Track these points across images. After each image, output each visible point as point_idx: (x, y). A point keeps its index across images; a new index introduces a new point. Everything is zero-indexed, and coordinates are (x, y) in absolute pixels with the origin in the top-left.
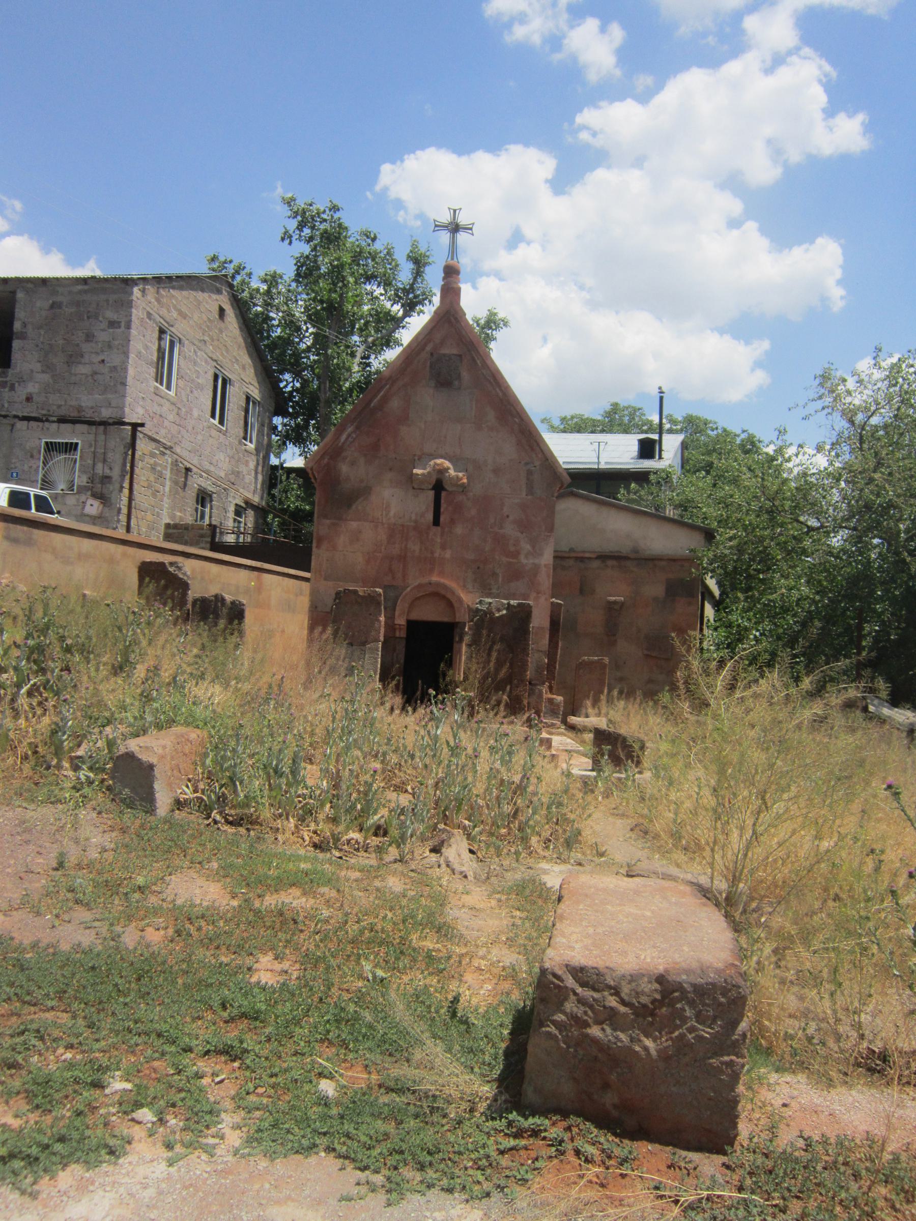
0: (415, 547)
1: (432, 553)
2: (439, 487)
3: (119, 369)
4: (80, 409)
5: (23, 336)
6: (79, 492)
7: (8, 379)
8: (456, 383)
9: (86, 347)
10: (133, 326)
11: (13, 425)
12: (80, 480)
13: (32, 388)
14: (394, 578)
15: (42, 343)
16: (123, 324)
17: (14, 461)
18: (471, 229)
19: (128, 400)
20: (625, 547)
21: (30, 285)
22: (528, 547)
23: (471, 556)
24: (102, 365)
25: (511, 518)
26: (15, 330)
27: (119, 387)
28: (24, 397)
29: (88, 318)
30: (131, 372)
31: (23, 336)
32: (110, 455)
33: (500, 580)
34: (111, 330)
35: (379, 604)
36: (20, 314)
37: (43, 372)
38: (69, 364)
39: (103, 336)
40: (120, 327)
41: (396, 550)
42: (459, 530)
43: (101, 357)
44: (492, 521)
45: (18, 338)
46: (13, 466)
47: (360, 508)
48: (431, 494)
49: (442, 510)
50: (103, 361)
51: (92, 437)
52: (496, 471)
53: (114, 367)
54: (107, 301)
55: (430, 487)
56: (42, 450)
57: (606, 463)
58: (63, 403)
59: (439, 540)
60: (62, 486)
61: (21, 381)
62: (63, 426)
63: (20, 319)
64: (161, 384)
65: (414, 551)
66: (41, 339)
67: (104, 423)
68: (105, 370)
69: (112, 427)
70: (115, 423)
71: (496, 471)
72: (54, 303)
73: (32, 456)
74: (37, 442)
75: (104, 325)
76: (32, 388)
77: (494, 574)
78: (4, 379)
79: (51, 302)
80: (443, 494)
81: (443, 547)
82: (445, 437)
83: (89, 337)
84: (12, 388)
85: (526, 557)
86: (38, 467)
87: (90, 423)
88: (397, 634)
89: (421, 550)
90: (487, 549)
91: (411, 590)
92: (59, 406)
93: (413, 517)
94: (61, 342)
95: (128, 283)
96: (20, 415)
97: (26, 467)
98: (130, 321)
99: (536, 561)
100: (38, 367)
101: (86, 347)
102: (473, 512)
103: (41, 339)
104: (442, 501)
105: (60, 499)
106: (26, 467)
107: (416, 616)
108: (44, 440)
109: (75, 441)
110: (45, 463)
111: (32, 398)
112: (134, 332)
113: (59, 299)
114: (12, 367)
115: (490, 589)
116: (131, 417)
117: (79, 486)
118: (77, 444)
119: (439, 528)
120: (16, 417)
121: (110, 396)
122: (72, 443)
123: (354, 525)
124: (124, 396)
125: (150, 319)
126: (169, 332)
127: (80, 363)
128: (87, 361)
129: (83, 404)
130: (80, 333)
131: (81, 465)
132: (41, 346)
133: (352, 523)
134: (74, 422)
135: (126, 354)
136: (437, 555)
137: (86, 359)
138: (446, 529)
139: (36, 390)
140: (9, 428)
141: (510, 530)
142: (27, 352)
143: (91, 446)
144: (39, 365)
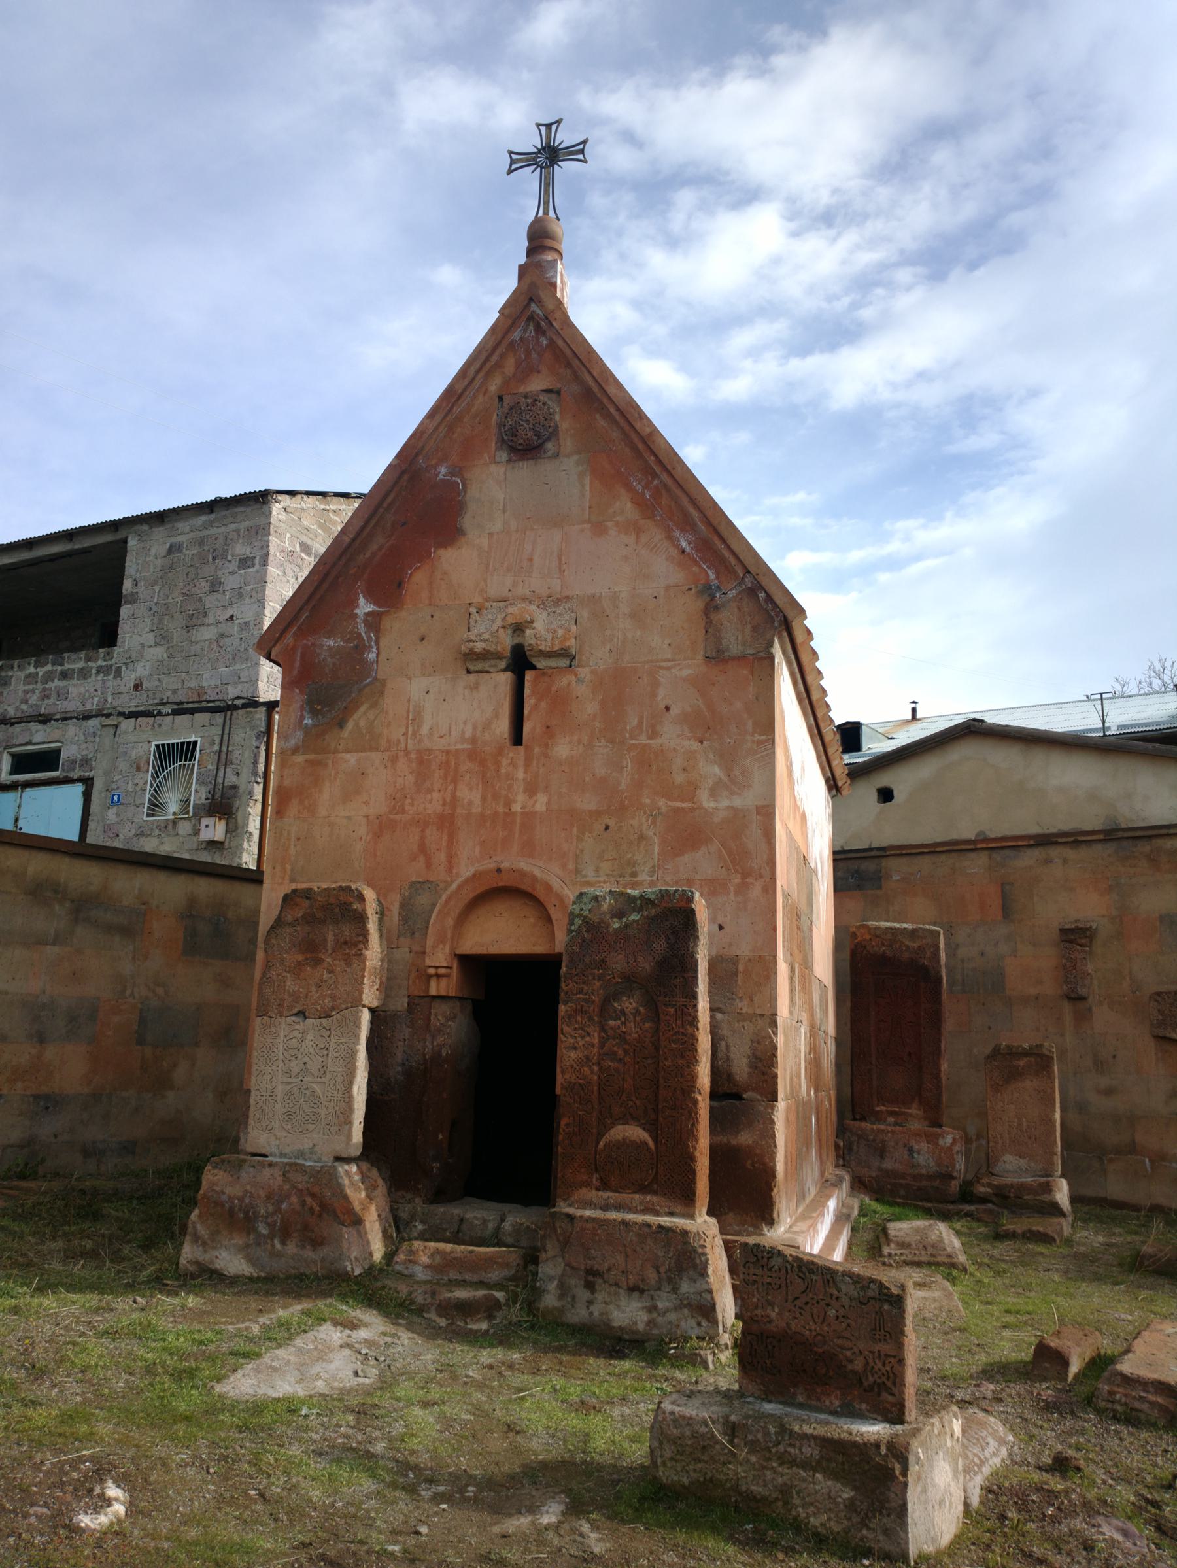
0: (471, 795)
1: (508, 803)
3: (251, 624)
4: (200, 691)
5: (133, 599)
6: (195, 814)
7: (113, 661)
8: (549, 445)
9: (211, 601)
10: (271, 558)
11: (116, 726)
12: (198, 795)
13: (141, 670)
14: (428, 865)
15: (156, 604)
16: (257, 561)
17: (116, 778)
18: (582, 152)
20: (1091, 820)
21: (145, 527)
22: (716, 770)
23: (588, 802)
24: (229, 623)
25: (674, 711)
26: (124, 592)
28: (132, 685)
29: (214, 559)
31: (133, 599)
32: (236, 753)
33: (656, 850)
34: (242, 572)
35: (361, 918)
36: (131, 566)
37: (157, 644)
39: (231, 582)
41: (432, 804)
42: (563, 749)
45: (127, 603)
46: (114, 786)
47: (362, 723)
48: (505, 680)
49: (526, 712)
50: (232, 617)
51: (216, 731)
52: (638, 616)
53: (245, 623)
54: (238, 531)
55: (503, 664)
56: (152, 758)
57: (1119, 727)
59: (520, 774)
60: (173, 807)
61: (130, 662)
62: (178, 718)
63: (131, 577)
65: (470, 803)
66: (155, 600)
68: (234, 629)
69: (240, 712)
70: (245, 706)
71: (638, 616)
72: (171, 546)
73: (138, 769)
74: (146, 746)
75: (233, 566)
76: (141, 670)
77: (642, 837)
78: (109, 663)
79: (168, 545)
80: (529, 676)
81: (531, 790)
82: (531, 560)
83: (215, 586)
84: (118, 673)
85: (713, 794)
86: (146, 782)
87: (214, 710)
88: (433, 991)
89: (484, 799)
90: (623, 786)
91: (460, 887)
92: (175, 692)
93: (469, 733)
95: (261, 498)
96: (126, 711)
97: (130, 787)
98: (267, 554)
99: (737, 802)
100: (150, 638)
101: (211, 601)
102: (591, 708)
103: (155, 600)
104: (527, 691)
105: (170, 827)
106: (130, 787)
108: (153, 744)
109: (193, 739)
110: (156, 775)
111: (141, 684)
113: (179, 539)
114: (119, 644)
115: (634, 874)
117: (194, 804)
118: (195, 743)
119: (521, 749)
120: (121, 714)
121: (238, 667)
122: (189, 743)
123: (351, 759)
128: (211, 621)
129: (205, 684)
130: (203, 584)
131: (199, 773)
132: (155, 609)
133: (348, 756)
134: (192, 711)
136: (517, 808)
137: (210, 619)
138: (537, 750)
139: (146, 673)
140: (112, 731)
142: (137, 620)
143: (213, 743)
144: (151, 635)
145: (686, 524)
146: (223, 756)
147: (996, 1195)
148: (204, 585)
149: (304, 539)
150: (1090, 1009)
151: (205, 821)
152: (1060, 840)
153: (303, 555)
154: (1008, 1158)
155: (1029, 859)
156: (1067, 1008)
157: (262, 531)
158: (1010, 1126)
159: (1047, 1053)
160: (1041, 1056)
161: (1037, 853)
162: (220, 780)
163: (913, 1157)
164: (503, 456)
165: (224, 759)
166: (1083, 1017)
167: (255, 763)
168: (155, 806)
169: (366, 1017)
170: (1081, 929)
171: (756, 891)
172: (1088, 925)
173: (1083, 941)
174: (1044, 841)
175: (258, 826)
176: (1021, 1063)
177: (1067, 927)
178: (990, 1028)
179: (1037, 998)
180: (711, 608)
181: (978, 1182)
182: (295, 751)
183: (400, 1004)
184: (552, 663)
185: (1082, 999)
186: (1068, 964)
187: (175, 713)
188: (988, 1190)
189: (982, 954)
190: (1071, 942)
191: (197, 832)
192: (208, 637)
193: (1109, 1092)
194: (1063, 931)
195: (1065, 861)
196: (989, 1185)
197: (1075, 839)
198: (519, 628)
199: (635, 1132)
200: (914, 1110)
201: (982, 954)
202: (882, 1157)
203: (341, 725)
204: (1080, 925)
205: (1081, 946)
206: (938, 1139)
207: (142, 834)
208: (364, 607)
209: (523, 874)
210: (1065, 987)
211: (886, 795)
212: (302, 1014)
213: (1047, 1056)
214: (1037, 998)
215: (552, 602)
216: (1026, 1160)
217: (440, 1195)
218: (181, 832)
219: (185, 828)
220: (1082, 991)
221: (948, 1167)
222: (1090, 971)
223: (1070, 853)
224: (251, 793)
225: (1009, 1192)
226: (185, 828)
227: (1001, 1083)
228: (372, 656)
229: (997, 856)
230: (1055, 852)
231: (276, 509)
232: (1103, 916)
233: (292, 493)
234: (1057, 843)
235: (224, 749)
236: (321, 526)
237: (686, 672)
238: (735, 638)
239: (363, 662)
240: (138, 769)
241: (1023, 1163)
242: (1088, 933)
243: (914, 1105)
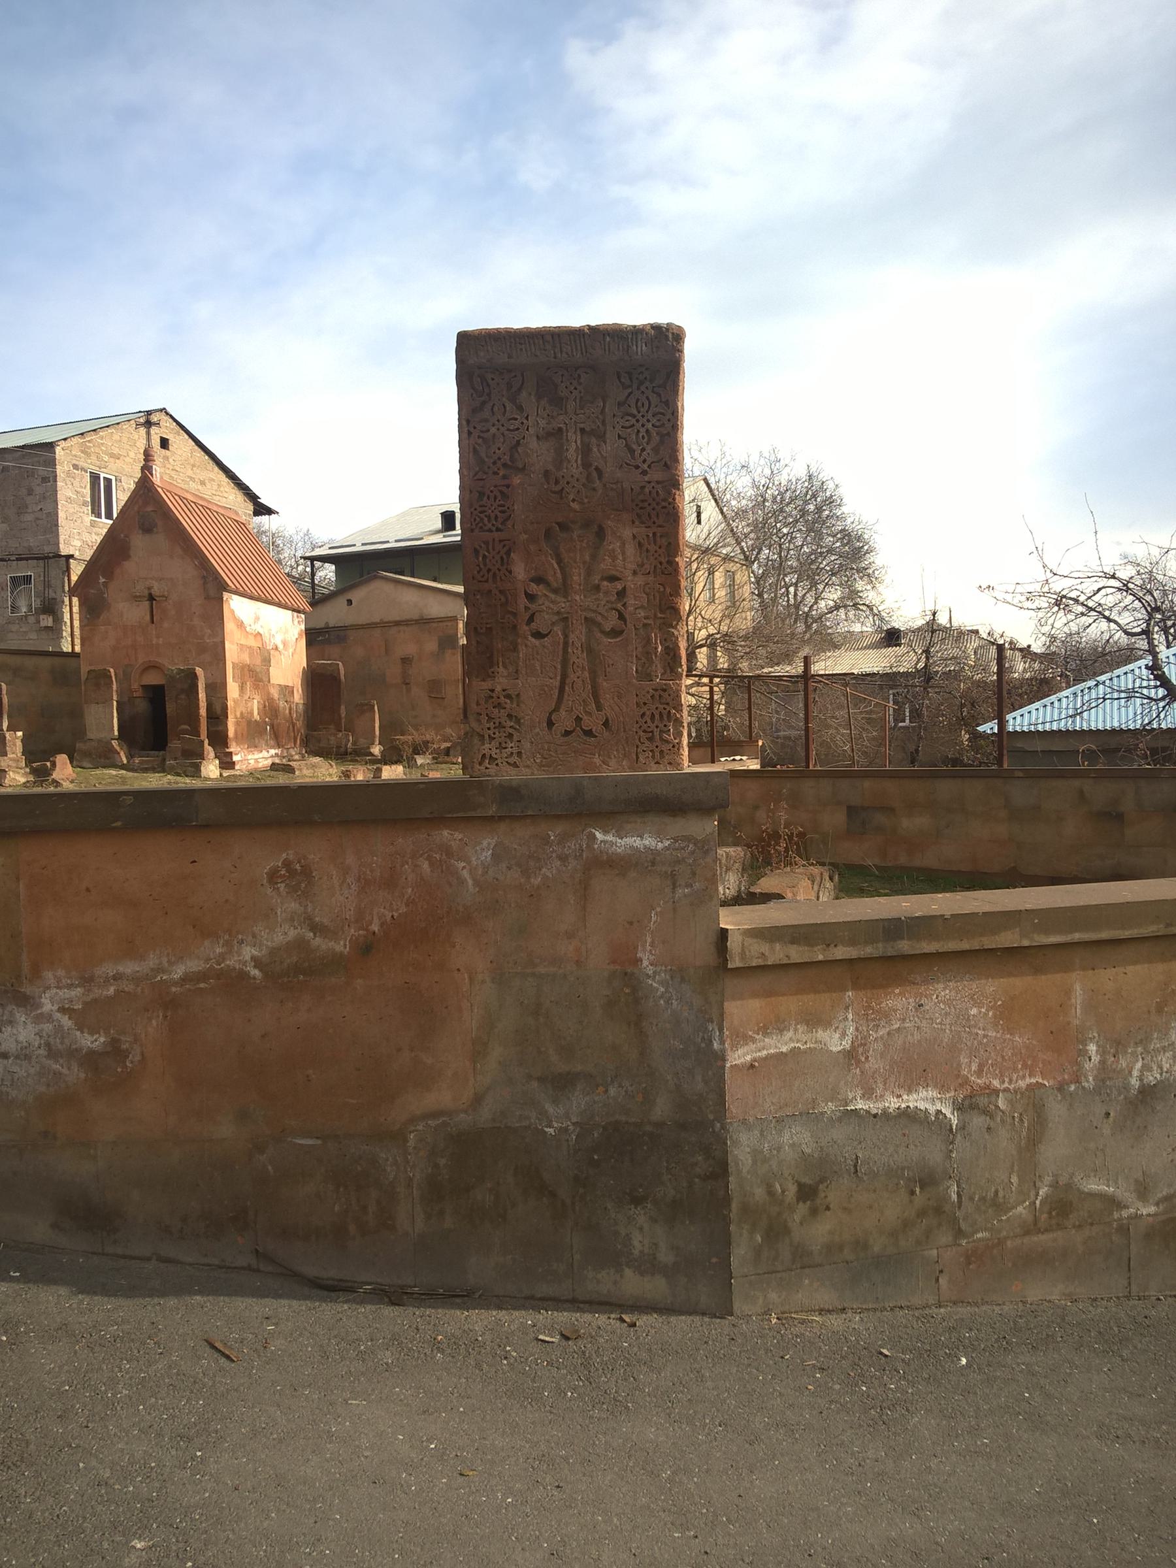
2: (151, 598)
4: (30, 548)
9: (29, 500)
12: (36, 603)
19: (62, 538)
22: (209, 631)
25: (197, 614)
27: (54, 528)
30: (61, 515)
32: (53, 582)
38: (19, 514)
39: (38, 490)
40: (49, 482)
42: (166, 625)
43: (40, 507)
44: (185, 617)
50: (41, 509)
58: (18, 545)
60: (24, 610)
64: (99, 516)
67: (48, 558)
69: (53, 560)
70: (54, 557)
80: (154, 602)
81: (158, 637)
83: (30, 492)
87: (37, 559)
94: (12, 498)
95: (50, 446)
98: (56, 476)
99: (215, 640)
101: (29, 500)
107: (144, 683)
109: (29, 574)
110: (12, 593)
112: (59, 484)
116: (64, 550)
118: (31, 576)
124: (58, 535)
125: (78, 470)
126: (102, 475)
127: (26, 513)
133: (102, 627)
134: (27, 559)
135: (56, 502)
136: (154, 642)
141: (196, 621)
143: (40, 576)
145: (196, 557)
146: (47, 583)
148: (24, 491)
149: (74, 462)
151: (42, 617)
153: (75, 471)
155: (394, 630)
156: (404, 687)
157: (52, 463)
162: (47, 595)
164: (141, 532)
165: (47, 584)
166: (409, 691)
167: (64, 586)
168: (14, 608)
169: (115, 703)
171: (221, 665)
174: (398, 623)
175: (69, 617)
176: (365, 708)
180: (205, 583)
182: (85, 626)
183: (126, 699)
184: (161, 598)
187: (17, 559)
191: (39, 622)
192: (29, 519)
193: (416, 717)
197: (406, 623)
198: (149, 589)
199: (186, 727)
200: (332, 727)
203: (99, 617)
207: (9, 622)
208: (102, 580)
209: (157, 662)
211: (350, 602)
212: (98, 703)
215: (160, 580)
217: (143, 749)
218: (30, 621)
219: (32, 620)
223: (405, 628)
224: (63, 602)
226: (32, 620)
228: (106, 596)
230: (402, 628)
231: (58, 450)
233: (65, 439)
235: (46, 579)
236: (82, 452)
237: (199, 602)
238: (212, 593)
239: (104, 598)
240: (2, 589)
241: (365, 741)
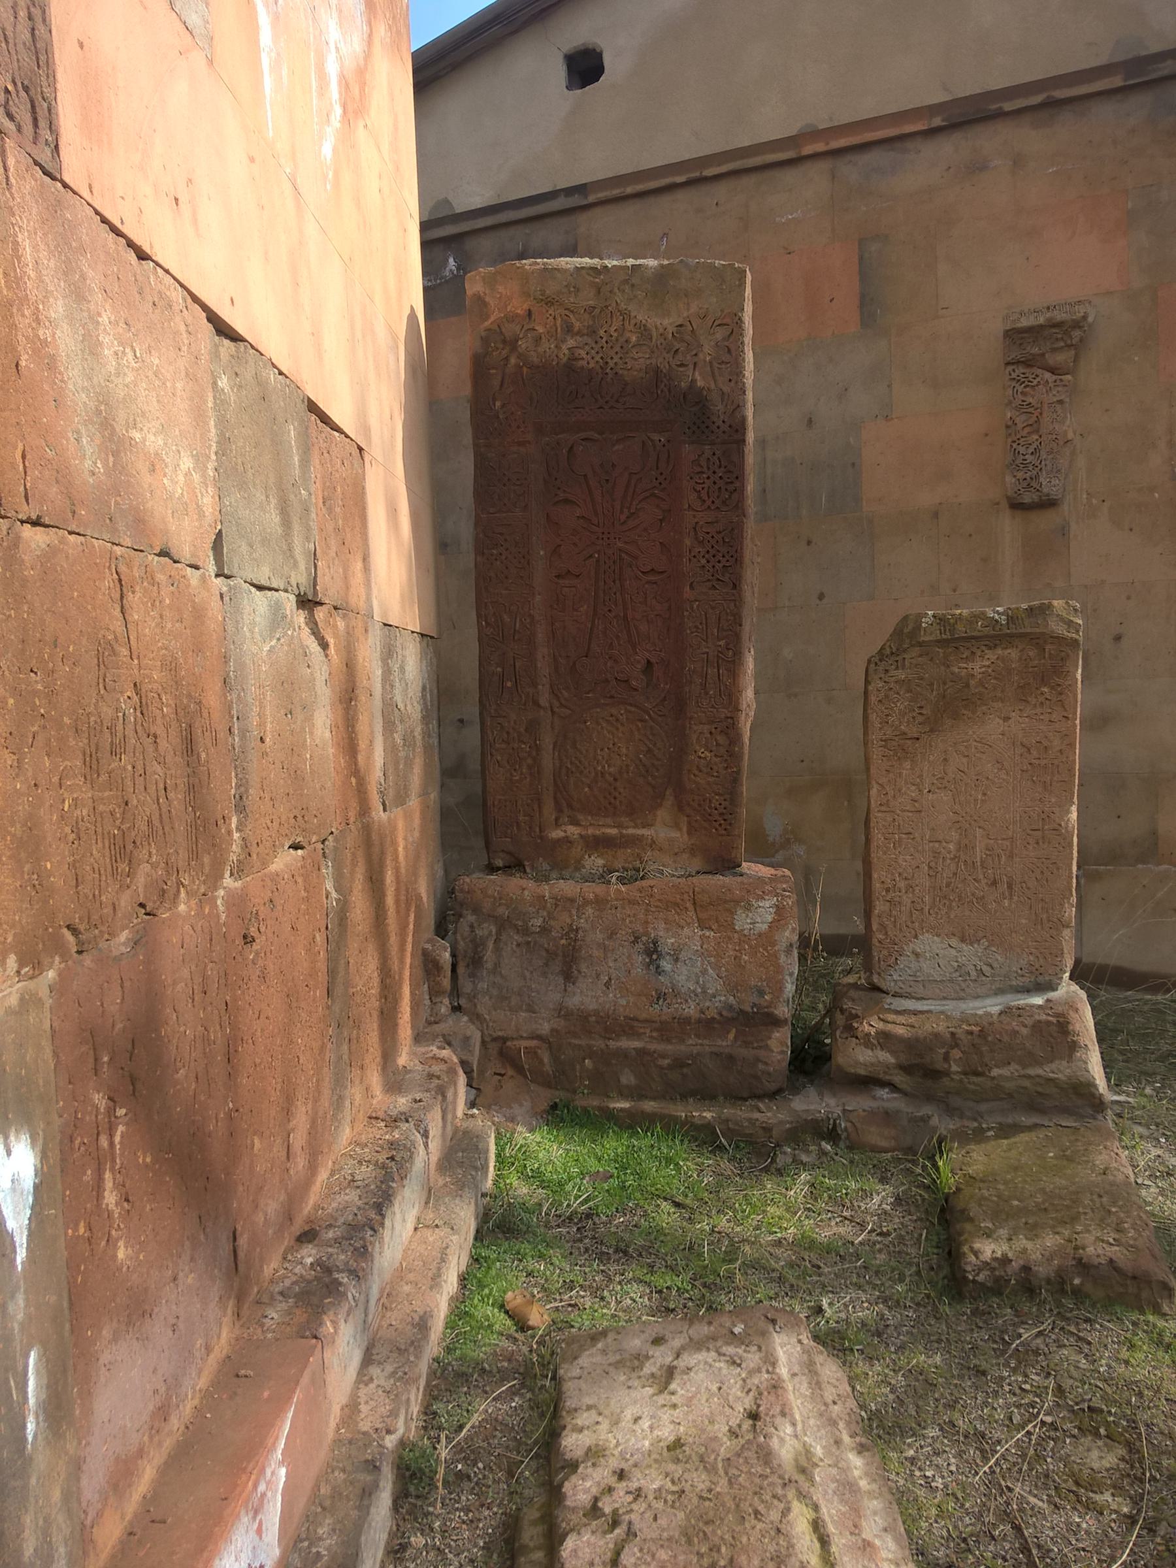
147: (906, 1069)
150: (1064, 531)
152: (1008, 106)
154: (928, 943)
156: (1008, 526)
158: (936, 854)
159: (1060, 630)
160: (1038, 640)
161: (948, 149)
163: (659, 971)
170: (1059, 325)
172: (1080, 312)
173: (1060, 358)
177: (1025, 323)
178: (821, 597)
179: (936, 515)
181: (850, 1030)
185: (1049, 503)
186: (1020, 420)
188: (885, 1057)
189: (810, 421)
190: (1028, 363)
194: (1014, 335)
195: (1018, 162)
196: (885, 1039)
201: (810, 421)
202: (568, 976)
204: (1059, 316)
205: (1053, 371)
206: (732, 913)
210: (1009, 479)
213: (1059, 640)
214: (936, 515)
216: (979, 949)
220: (1049, 486)
221: (761, 993)
222: (1070, 435)
225: (946, 1058)
227: (913, 731)
229: (851, 170)
232: (1109, 293)
234: (1001, 115)
241: (970, 955)
242: (1076, 334)
243: (663, 814)
